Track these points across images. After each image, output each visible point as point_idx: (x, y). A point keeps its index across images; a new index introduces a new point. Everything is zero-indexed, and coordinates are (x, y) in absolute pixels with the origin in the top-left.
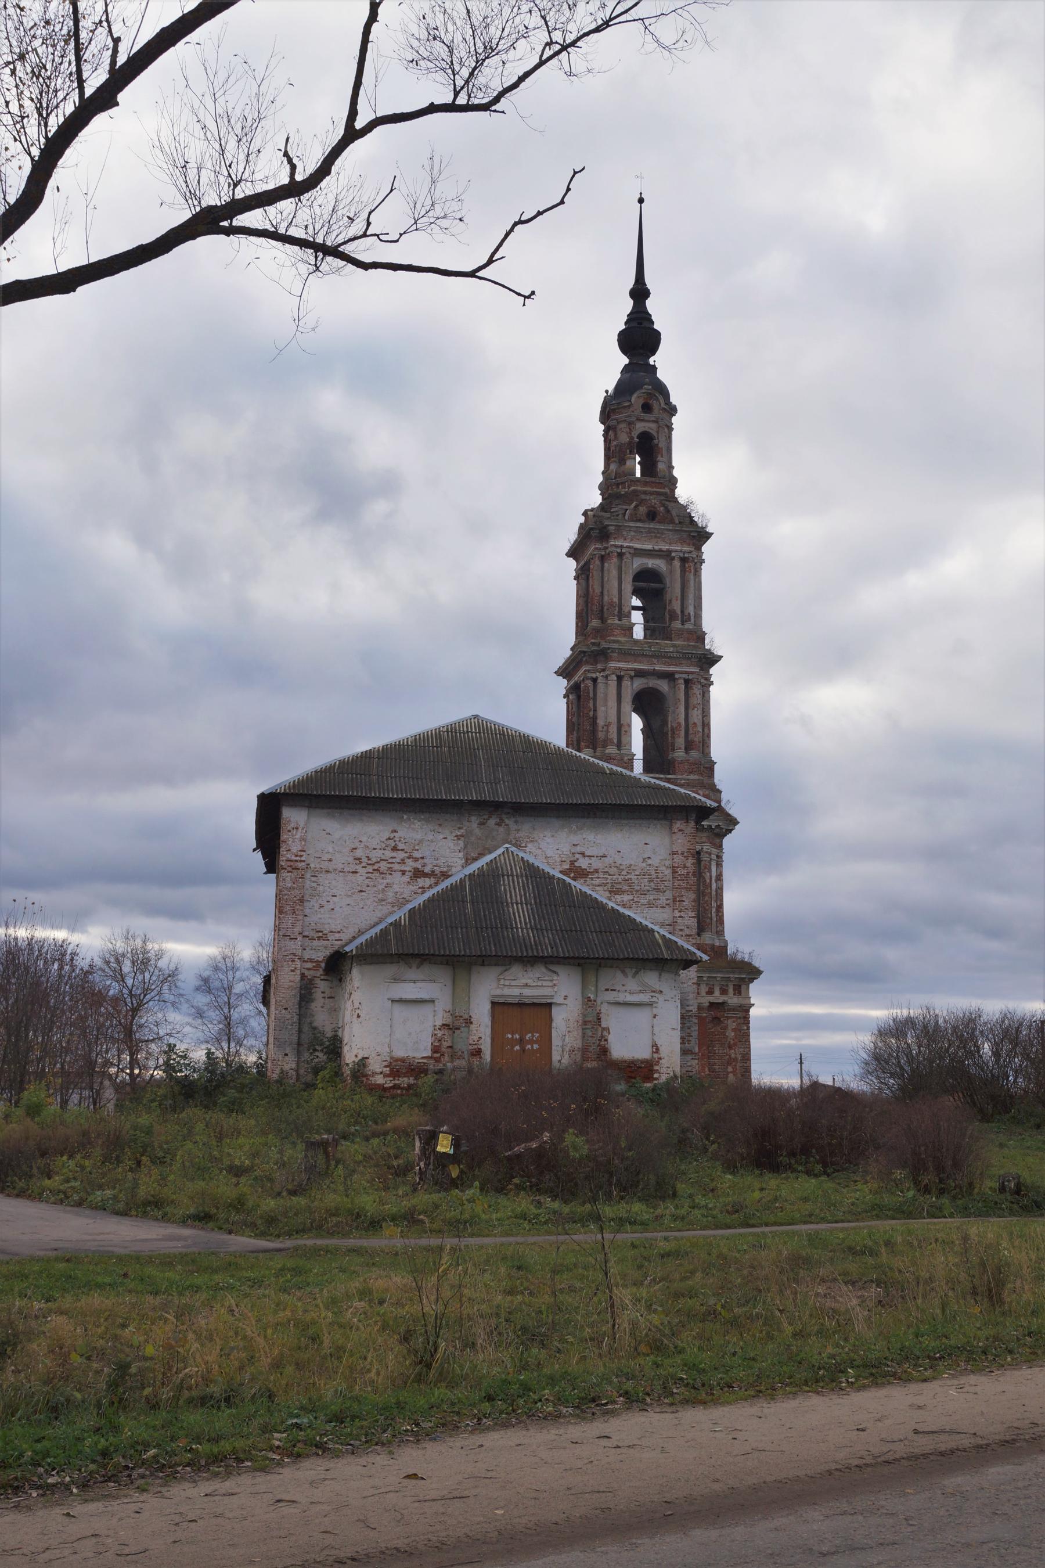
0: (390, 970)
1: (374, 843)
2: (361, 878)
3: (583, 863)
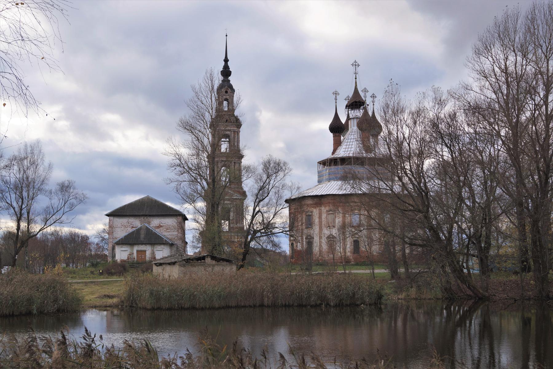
0: (121, 246)
2: (123, 228)
3: (162, 225)
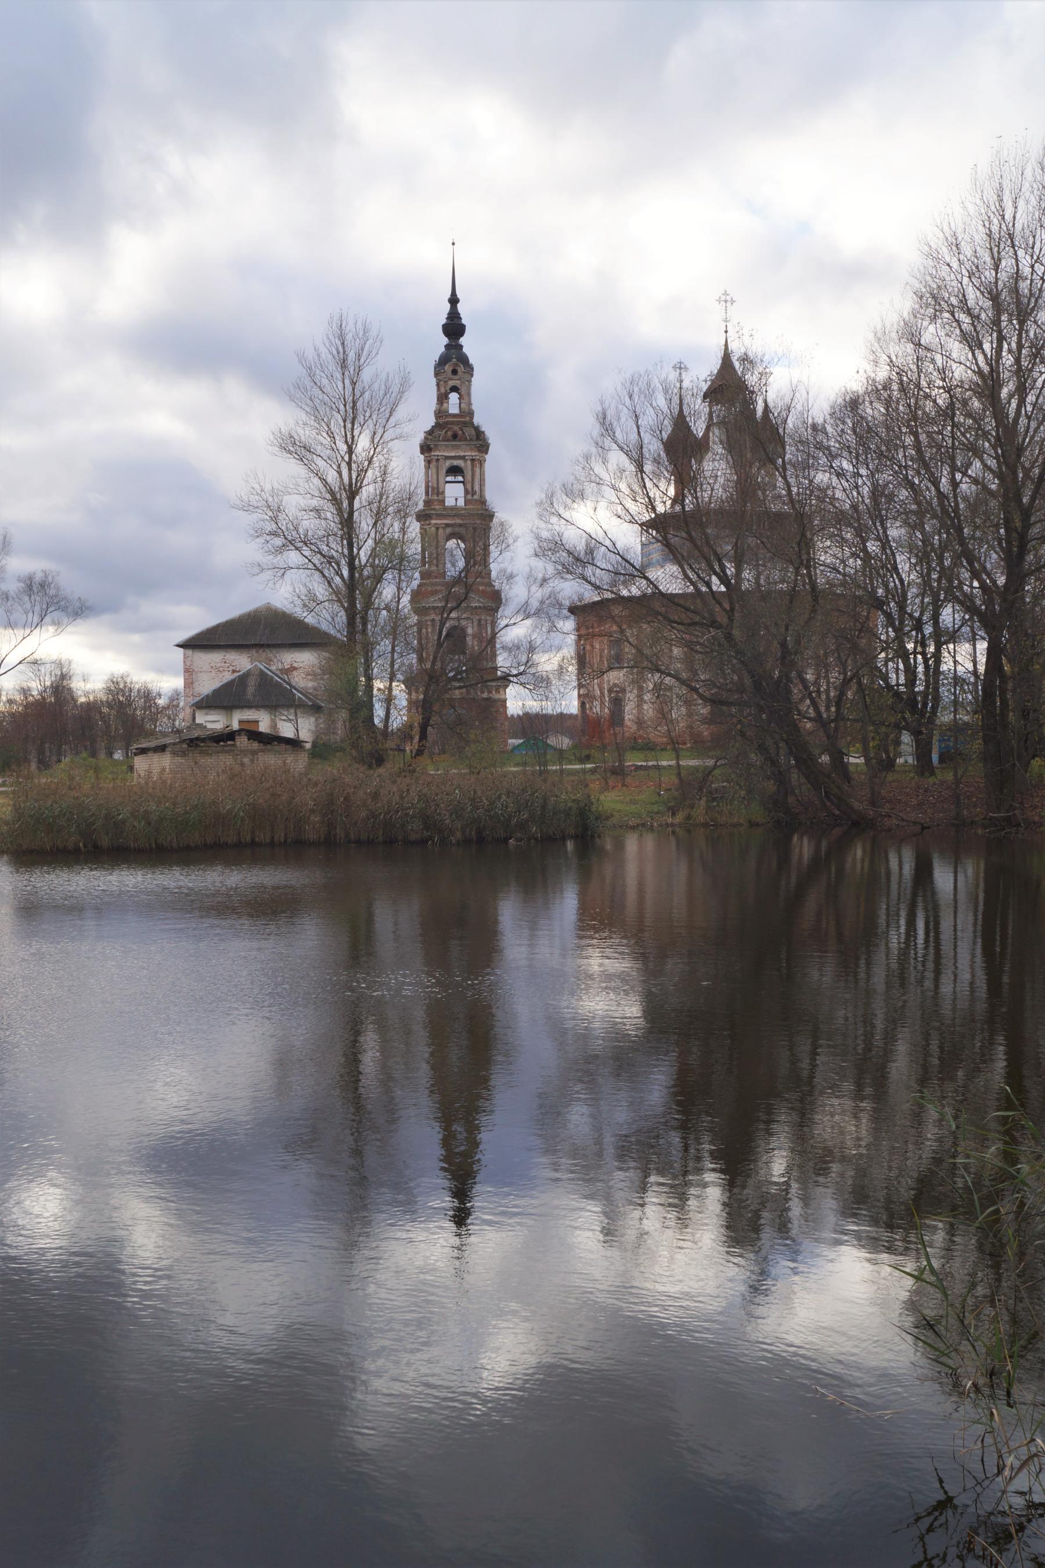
1: (218, 660)
3: (295, 665)
